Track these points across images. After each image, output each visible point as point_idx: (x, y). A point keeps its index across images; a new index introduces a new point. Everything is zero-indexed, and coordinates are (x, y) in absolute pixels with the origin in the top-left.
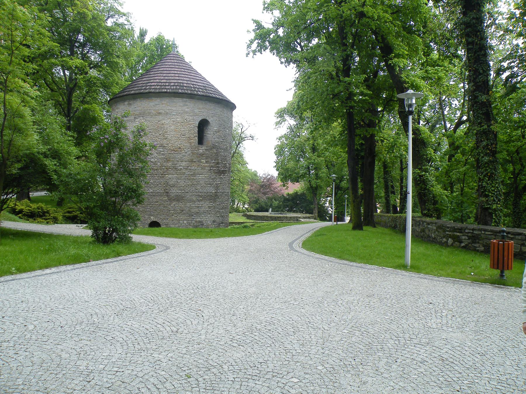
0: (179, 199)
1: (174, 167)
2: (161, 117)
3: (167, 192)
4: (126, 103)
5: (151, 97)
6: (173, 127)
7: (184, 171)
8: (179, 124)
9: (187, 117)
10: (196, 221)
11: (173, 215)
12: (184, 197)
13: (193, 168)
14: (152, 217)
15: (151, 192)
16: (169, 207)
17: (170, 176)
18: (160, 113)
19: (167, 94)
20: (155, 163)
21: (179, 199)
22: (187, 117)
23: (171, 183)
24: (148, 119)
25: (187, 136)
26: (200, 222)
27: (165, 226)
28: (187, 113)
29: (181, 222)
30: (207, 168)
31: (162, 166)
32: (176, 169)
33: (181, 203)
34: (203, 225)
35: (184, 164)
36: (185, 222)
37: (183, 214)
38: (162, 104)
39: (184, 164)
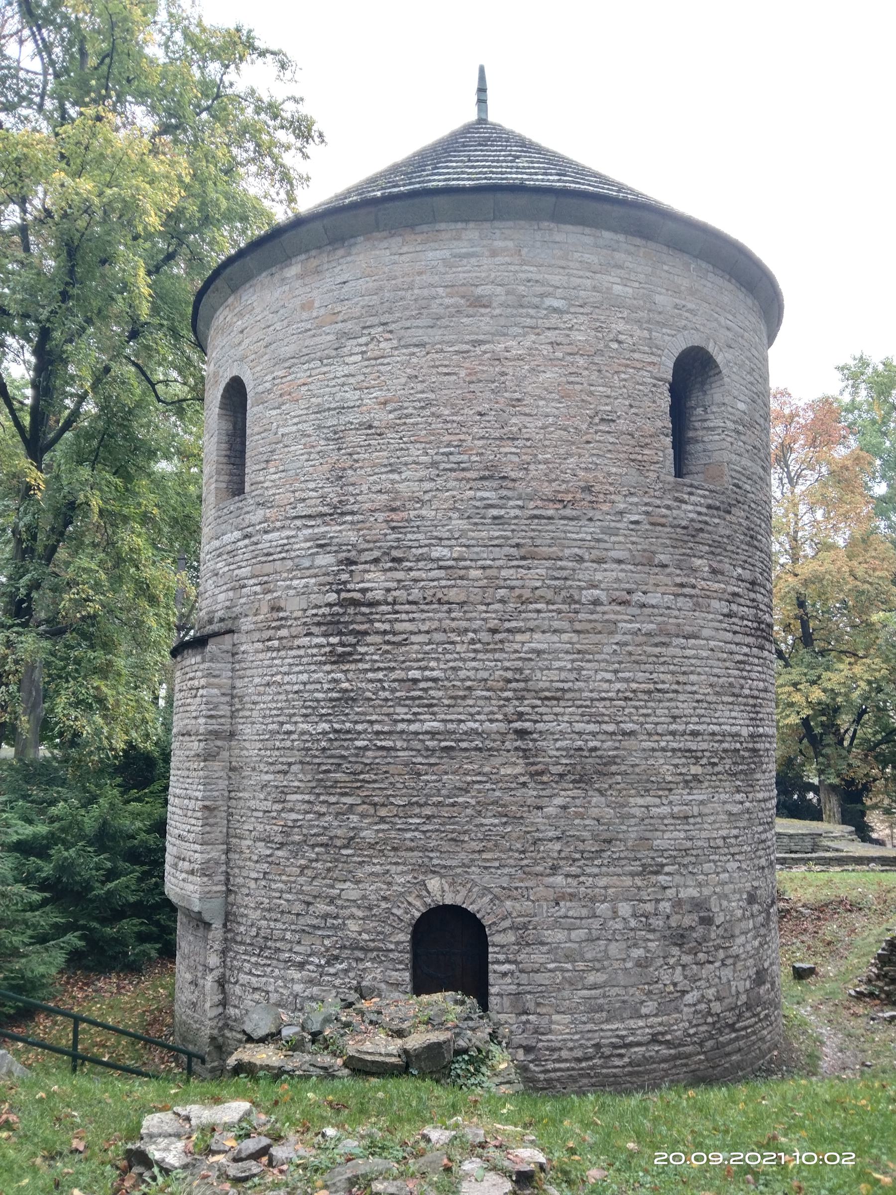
0: (588, 772)
1: (557, 590)
2: (484, 323)
3: (522, 734)
4: (293, 270)
5: (434, 218)
6: (550, 375)
7: (611, 612)
8: (581, 361)
9: (621, 326)
10: (678, 903)
11: (555, 869)
12: (613, 761)
13: (652, 599)
14: (433, 883)
15: (433, 734)
16: (537, 818)
17: (539, 641)
18: (479, 303)
19: (522, 200)
20: (453, 570)
21: (588, 772)
22: (621, 326)
23: (543, 680)
24: (420, 335)
25: (622, 425)
26: (698, 905)
27: (510, 937)
28: (617, 304)
29: (603, 908)
30: (715, 604)
31: (493, 582)
32: (571, 600)
33: (596, 799)
34: (707, 921)
35: (608, 574)
36: (625, 909)
37: (613, 862)
38: (494, 253)
39: (608, 574)
